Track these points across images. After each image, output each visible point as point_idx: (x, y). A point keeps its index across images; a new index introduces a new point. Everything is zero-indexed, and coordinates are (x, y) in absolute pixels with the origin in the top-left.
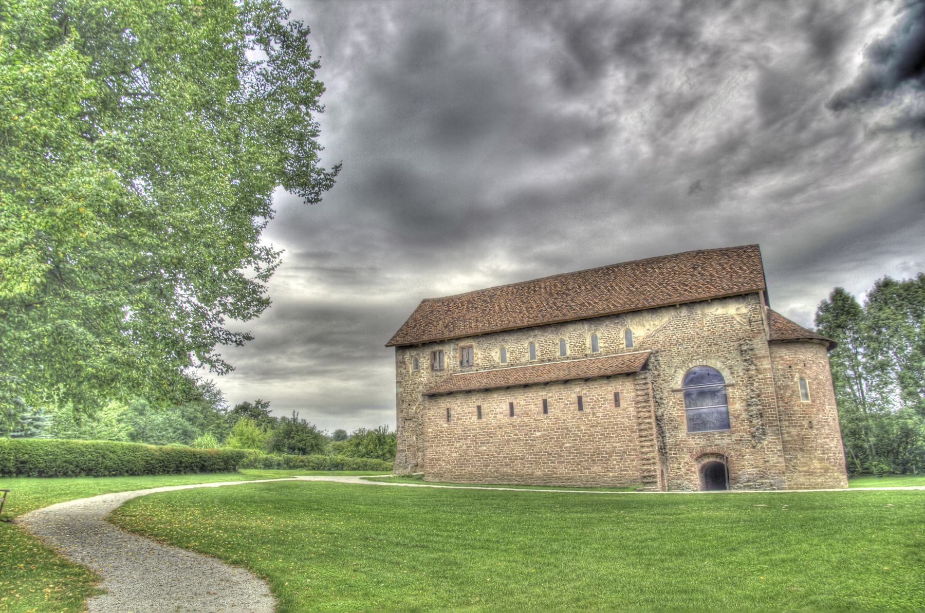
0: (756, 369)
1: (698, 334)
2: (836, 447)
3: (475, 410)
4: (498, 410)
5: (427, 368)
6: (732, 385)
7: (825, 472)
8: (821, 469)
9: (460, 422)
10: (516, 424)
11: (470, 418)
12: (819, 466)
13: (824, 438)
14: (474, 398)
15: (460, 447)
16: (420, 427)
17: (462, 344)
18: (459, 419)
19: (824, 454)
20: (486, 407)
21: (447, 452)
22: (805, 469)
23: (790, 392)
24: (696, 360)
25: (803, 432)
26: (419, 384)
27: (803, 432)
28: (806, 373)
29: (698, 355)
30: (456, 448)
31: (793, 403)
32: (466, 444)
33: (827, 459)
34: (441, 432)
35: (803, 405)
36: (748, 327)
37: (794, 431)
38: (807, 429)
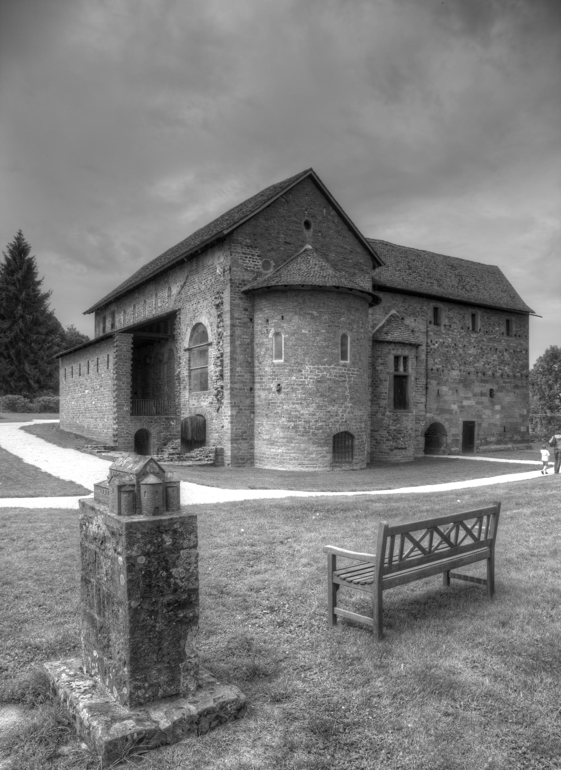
0: (223, 326)
1: (200, 289)
2: (314, 415)
6: (210, 344)
7: (287, 442)
8: (284, 438)
12: (281, 435)
13: (293, 404)
19: (289, 422)
22: (267, 437)
23: (264, 350)
24: (197, 317)
25: (270, 396)
27: (270, 396)
28: (282, 327)
29: (198, 311)
31: (265, 363)
33: (293, 428)
35: (274, 366)
36: (222, 278)
37: (263, 394)
38: (274, 393)
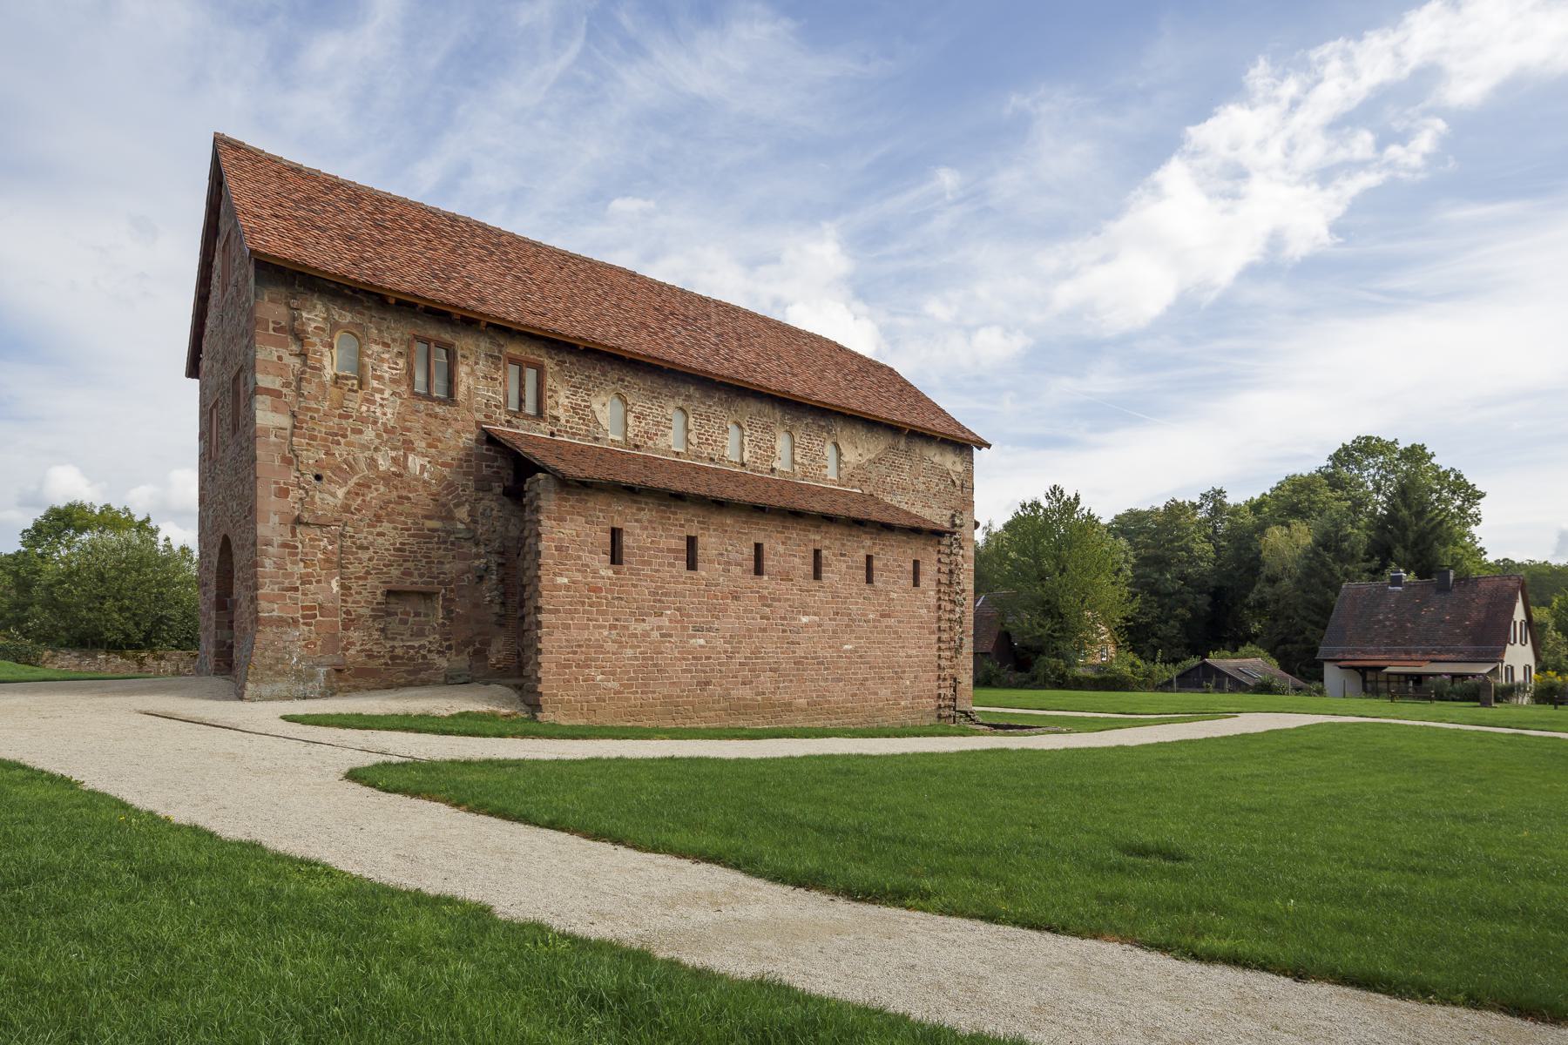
3: (683, 545)
4: (733, 555)
5: (393, 381)
9: (647, 570)
10: (765, 592)
11: (671, 565)
14: (682, 516)
15: (646, 634)
16: (364, 555)
17: (514, 349)
18: (644, 563)
20: (709, 543)
21: (609, 646)
26: (363, 420)
30: (635, 636)
32: (659, 628)
34: (597, 590)
